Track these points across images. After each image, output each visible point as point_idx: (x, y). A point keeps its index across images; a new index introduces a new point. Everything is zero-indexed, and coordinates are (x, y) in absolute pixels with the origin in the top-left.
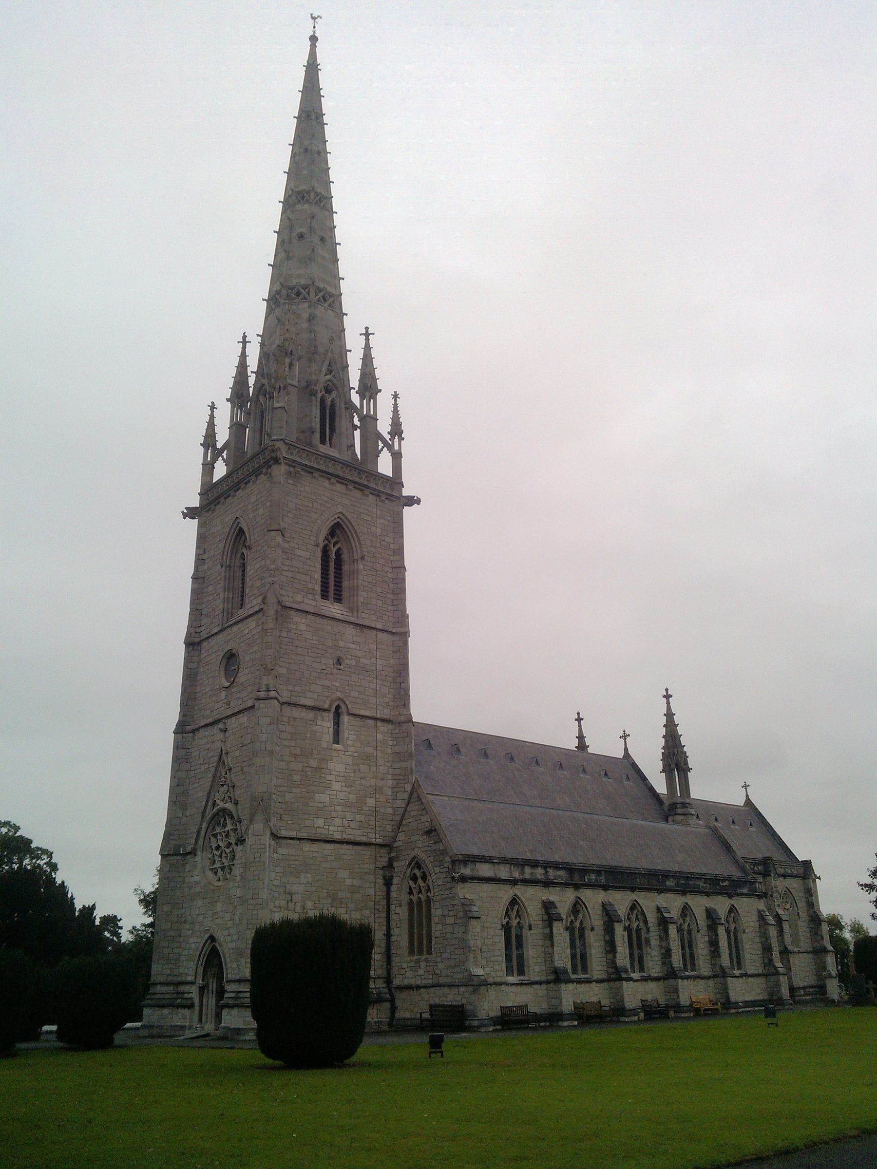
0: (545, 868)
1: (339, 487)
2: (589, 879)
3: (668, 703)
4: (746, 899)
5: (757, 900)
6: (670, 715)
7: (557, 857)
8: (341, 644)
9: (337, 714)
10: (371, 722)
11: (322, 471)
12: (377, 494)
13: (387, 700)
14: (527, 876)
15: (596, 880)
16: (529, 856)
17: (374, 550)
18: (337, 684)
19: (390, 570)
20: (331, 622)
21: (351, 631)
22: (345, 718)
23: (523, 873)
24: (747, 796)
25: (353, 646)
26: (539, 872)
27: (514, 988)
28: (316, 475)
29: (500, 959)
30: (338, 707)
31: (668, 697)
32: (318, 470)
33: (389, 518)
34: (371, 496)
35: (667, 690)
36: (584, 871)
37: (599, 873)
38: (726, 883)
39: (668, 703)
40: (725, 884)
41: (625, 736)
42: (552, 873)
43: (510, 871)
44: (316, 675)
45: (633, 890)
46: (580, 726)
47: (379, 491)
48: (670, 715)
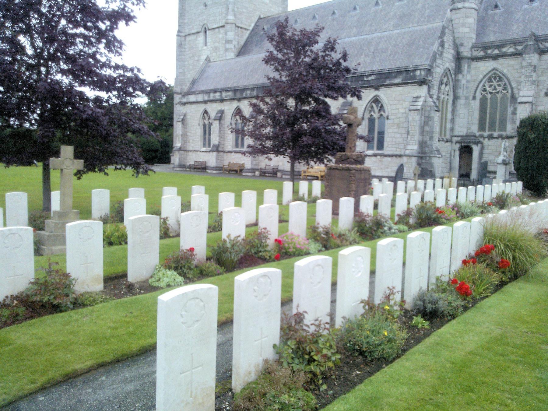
0: (221, 92)
2: (246, 94)
4: (400, 88)
5: (416, 87)
7: (230, 85)
9: (206, 32)
10: (217, 30)
14: (211, 98)
15: (251, 94)
16: (212, 87)
18: (204, 17)
22: (208, 32)
23: (209, 97)
26: (217, 96)
27: (203, 154)
29: (198, 140)
30: (205, 28)
36: (243, 90)
37: (253, 89)
38: (373, 77)
40: (370, 78)
42: (224, 94)
43: (203, 97)
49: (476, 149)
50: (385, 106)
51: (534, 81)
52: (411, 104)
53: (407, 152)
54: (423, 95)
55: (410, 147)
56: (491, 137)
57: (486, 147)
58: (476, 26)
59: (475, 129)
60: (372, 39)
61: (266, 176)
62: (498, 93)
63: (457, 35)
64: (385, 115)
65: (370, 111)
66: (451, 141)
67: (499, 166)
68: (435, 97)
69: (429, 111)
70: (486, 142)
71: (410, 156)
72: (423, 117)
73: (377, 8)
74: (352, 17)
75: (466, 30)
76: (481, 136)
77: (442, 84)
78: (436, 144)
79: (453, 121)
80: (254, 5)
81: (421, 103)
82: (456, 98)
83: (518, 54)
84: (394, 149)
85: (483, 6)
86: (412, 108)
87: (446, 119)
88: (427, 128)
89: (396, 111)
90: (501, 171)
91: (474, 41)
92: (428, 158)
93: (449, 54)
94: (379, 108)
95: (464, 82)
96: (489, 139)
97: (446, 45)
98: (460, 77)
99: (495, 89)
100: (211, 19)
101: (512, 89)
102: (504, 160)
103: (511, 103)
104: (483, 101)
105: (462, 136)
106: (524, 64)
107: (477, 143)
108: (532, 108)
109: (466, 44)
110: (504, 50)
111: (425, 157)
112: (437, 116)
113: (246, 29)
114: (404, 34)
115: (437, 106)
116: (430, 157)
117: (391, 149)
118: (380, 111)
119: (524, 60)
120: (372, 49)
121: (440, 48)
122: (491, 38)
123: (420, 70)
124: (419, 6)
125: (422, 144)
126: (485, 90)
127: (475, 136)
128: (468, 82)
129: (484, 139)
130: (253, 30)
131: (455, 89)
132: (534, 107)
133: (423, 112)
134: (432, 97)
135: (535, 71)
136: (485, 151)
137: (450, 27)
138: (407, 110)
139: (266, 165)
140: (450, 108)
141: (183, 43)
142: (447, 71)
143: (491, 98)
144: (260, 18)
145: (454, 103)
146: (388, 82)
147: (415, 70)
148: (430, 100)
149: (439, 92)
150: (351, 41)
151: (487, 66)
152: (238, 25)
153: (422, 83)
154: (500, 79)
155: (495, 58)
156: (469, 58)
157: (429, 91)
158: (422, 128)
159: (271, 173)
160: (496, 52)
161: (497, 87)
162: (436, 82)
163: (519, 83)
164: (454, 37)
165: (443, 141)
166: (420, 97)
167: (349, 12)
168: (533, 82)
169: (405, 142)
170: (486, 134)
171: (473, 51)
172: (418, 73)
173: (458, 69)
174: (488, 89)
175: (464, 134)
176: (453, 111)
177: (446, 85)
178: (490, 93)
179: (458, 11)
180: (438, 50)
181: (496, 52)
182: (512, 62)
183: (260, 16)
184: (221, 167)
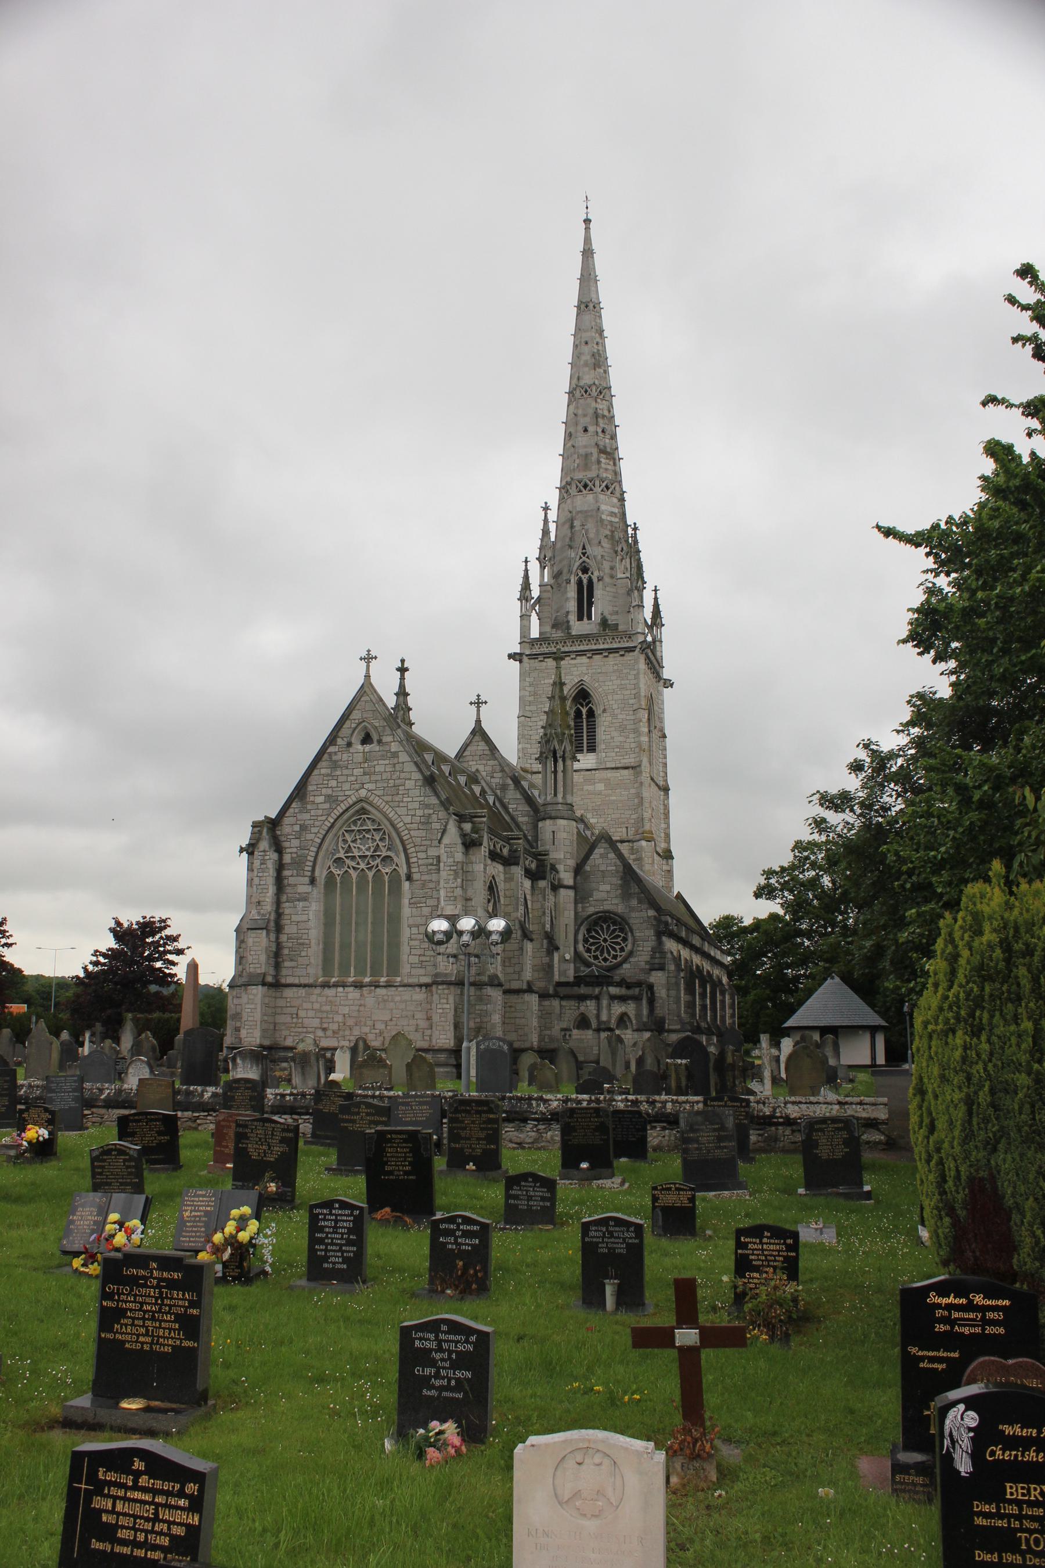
24: (367, 676)
31: (403, 670)
35: (403, 661)
39: (402, 678)
41: (478, 703)
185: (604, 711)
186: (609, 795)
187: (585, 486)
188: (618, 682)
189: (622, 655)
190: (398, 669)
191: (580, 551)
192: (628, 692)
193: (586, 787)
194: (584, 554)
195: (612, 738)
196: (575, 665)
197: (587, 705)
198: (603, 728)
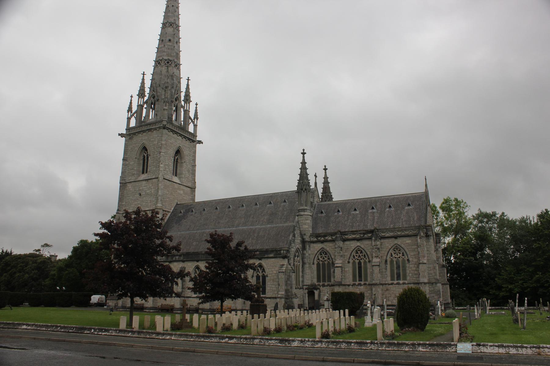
1: (144, 134)
2: (176, 259)
3: (304, 157)
4: (273, 260)
5: (281, 259)
6: (304, 163)
8: (141, 188)
11: (137, 132)
12: (155, 129)
13: (154, 202)
15: (179, 258)
17: (154, 150)
18: (139, 202)
19: (159, 155)
20: (138, 182)
21: (144, 183)
25: (145, 188)
28: (137, 134)
31: (304, 153)
32: (136, 132)
33: (160, 136)
34: (154, 131)
35: (304, 150)
39: (304, 157)
44: (133, 201)
45: (198, 261)
46: (326, 172)
47: (155, 128)
48: (304, 163)
49: (316, 293)
50: (265, 269)
51: (342, 256)
52: (279, 268)
53: (279, 296)
54: (286, 264)
55: (280, 293)
56: (324, 286)
57: (322, 291)
58: (311, 224)
59: (315, 281)
60: (256, 229)
61: (190, 313)
62: (325, 261)
63: (301, 229)
64: (266, 274)
65: (257, 272)
66: (303, 288)
67: (325, 302)
68: (292, 264)
69: (289, 273)
70: (321, 288)
71: (281, 298)
72: (286, 276)
73: (256, 206)
74: (241, 211)
75: (307, 226)
76: (319, 285)
77: (295, 256)
78: (294, 291)
79: (303, 276)
80: (173, 195)
81: (284, 268)
82: (304, 264)
83: (333, 241)
84: (272, 294)
85: (315, 211)
86: (280, 271)
87: (299, 276)
88: (289, 282)
89: (272, 272)
90: (327, 304)
91: (311, 232)
92: (290, 299)
93: (298, 240)
94: (262, 270)
95: (307, 255)
96: (323, 287)
97: (296, 236)
98: (305, 252)
99: (324, 259)
100: (144, 204)
101: (332, 259)
102: (327, 299)
103: (332, 266)
104: (318, 265)
105: (308, 285)
106: (336, 246)
107: (316, 289)
108: (342, 269)
109: (307, 234)
110: (326, 238)
111: (289, 298)
112: (293, 275)
113: (169, 212)
114: (273, 227)
115: (293, 270)
116: (291, 298)
117: (270, 294)
118: (262, 272)
119: (336, 244)
120: (256, 235)
121: (293, 238)
122: (320, 231)
123: (283, 250)
124: (281, 208)
125: (287, 291)
126: (319, 259)
127: (315, 285)
128: (309, 255)
129: (320, 287)
130: (173, 212)
131: (303, 259)
132: (343, 269)
133: (286, 273)
134: (290, 265)
135: (342, 251)
136: (321, 294)
137: (298, 226)
138: (278, 272)
139: (190, 305)
140: (301, 270)
141: (120, 218)
142: (298, 249)
143: (322, 264)
144: (177, 204)
145: (303, 266)
146: (266, 256)
147: (281, 250)
148: (289, 266)
149: (294, 261)
150: (243, 229)
151: (319, 246)
152: (164, 209)
153: (284, 257)
154: (326, 254)
155: (322, 242)
156: (309, 242)
157: (288, 261)
158: (286, 282)
159: (194, 311)
160: (322, 239)
161: (325, 258)
162: (292, 257)
163: (335, 256)
164: (300, 230)
165: (298, 288)
166: (284, 265)
167: (239, 207)
168: (342, 256)
169: (277, 290)
170: (321, 284)
171: (311, 238)
172: (282, 252)
173: (304, 248)
174: (320, 258)
175: (310, 284)
176: (303, 271)
177: (298, 257)
178: (322, 261)
179: (301, 216)
180: (292, 239)
181: (322, 239)
182: (331, 244)
183: (177, 203)
184: (156, 308)
185: (185, 162)
186: (184, 197)
187: (176, 66)
188: (189, 152)
189: (191, 142)
190: (302, 153)
191: (176, 92)
192: (191, 157)
193: (178, 191)
194: (177, 93)
195: (186, 174)
196: (178, 139)
197: (177, 156)
198: (184, 168)
